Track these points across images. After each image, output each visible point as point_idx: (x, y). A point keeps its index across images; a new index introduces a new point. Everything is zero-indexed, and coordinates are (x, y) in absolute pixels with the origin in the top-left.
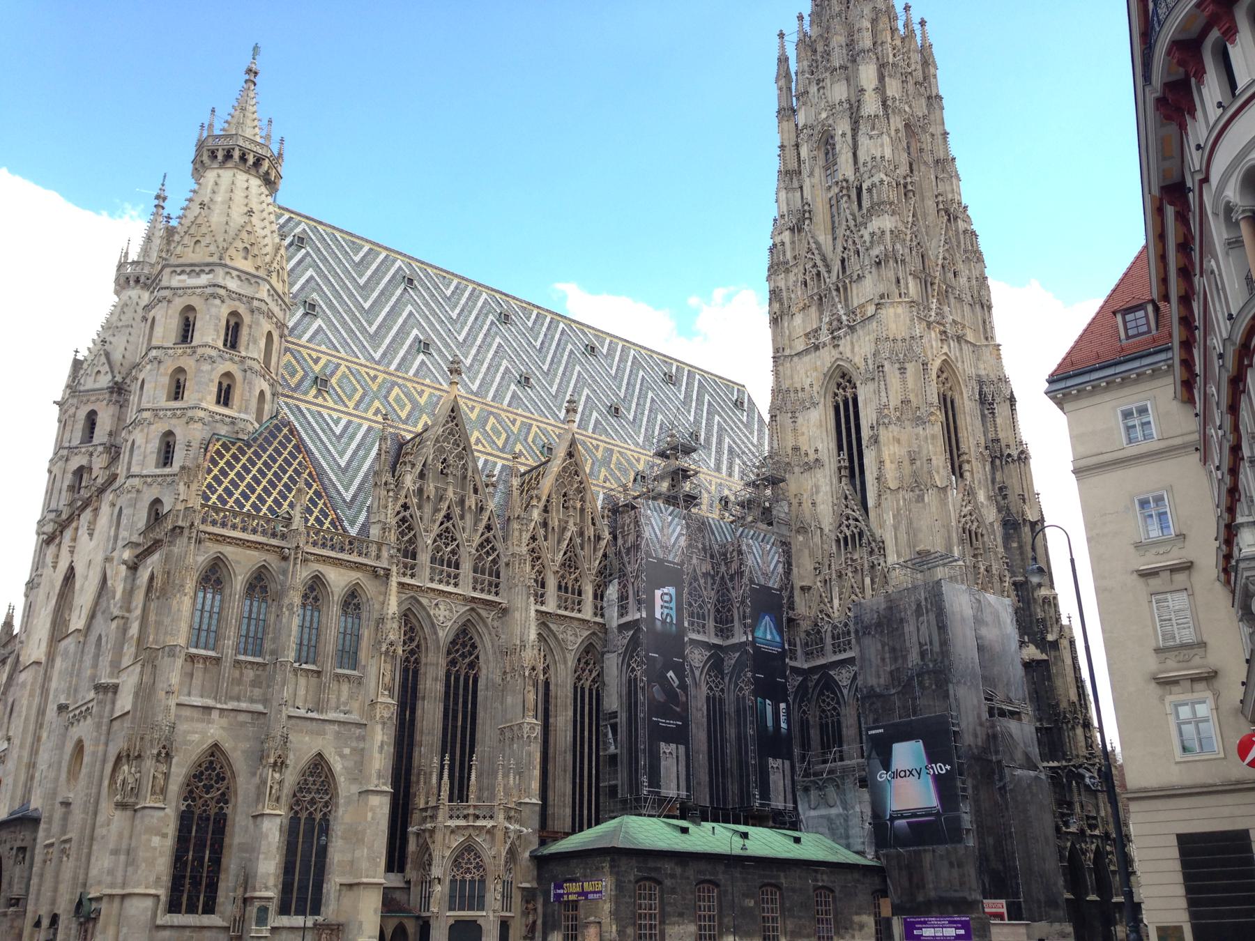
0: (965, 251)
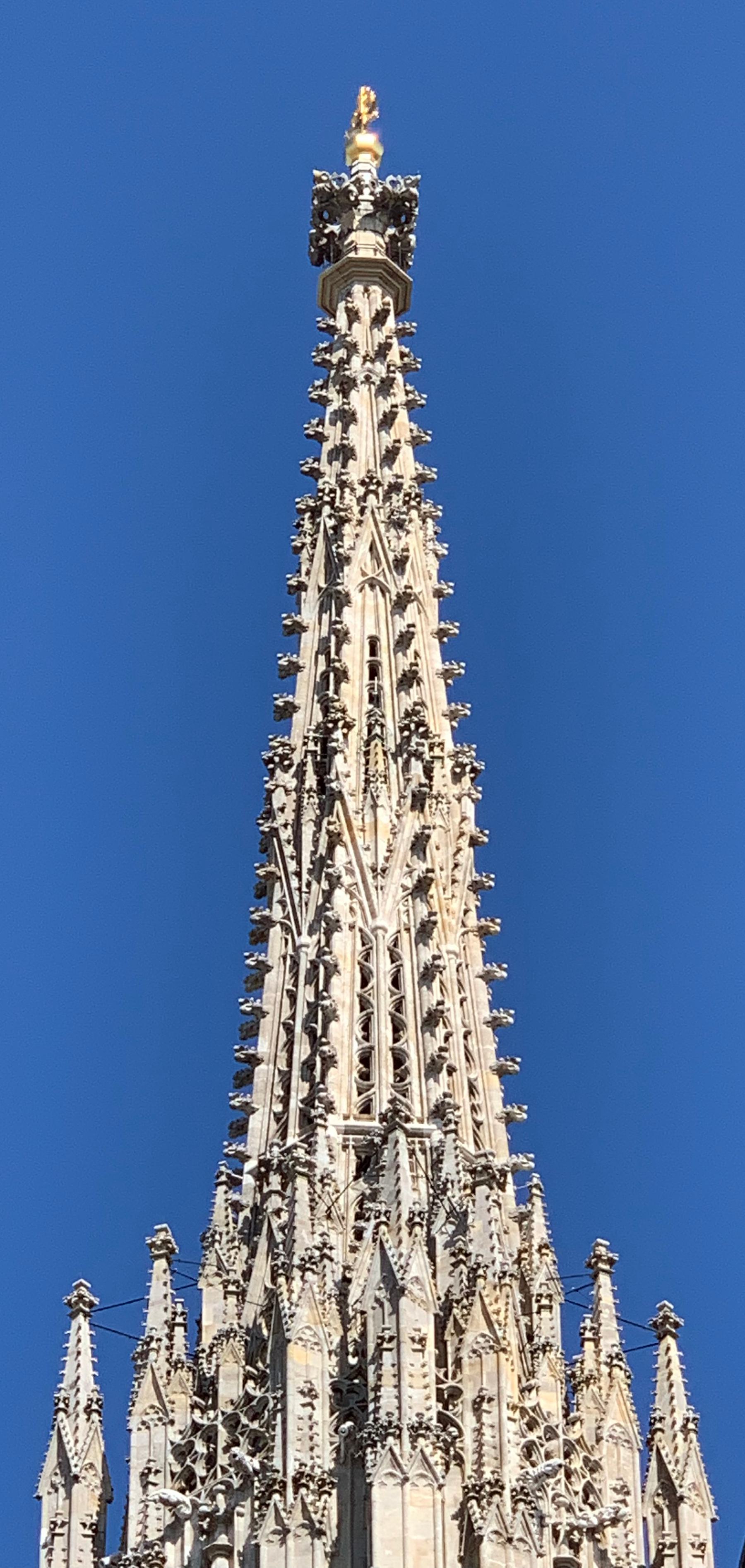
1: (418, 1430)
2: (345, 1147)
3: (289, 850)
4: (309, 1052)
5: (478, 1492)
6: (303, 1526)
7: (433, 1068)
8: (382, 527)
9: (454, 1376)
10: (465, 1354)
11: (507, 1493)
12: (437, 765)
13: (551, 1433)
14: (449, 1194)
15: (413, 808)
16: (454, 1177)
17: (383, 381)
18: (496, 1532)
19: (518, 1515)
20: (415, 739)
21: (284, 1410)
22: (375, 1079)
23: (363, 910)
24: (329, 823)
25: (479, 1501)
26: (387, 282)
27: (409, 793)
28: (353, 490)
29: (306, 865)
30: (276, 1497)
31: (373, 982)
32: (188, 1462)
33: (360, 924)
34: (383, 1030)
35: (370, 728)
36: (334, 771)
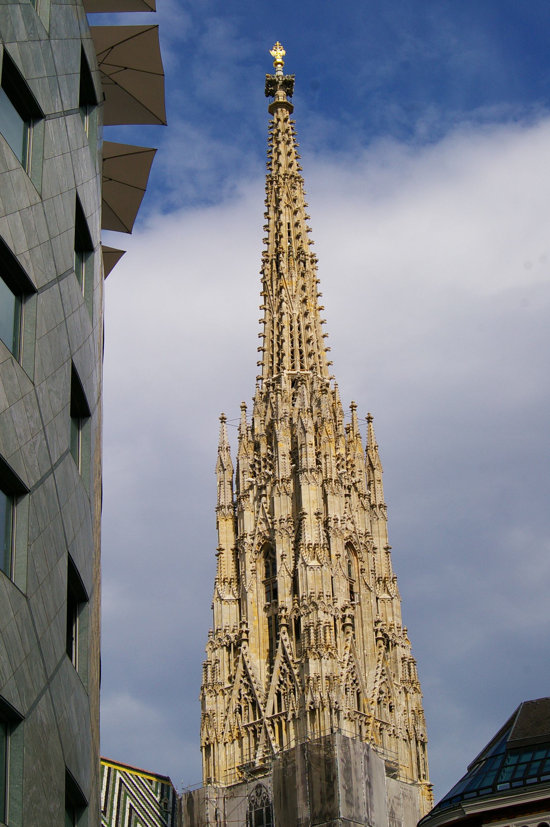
0: (402, 681)
1: (311, 470)
2: (288, 379)
3: (270, 288)
4: (278, 350)
5: (326, 481)
6: (284, 492)
7: (310, 355)
8: (290, 188)
9: (319, 448)
10: (321, 442)
11: (333, 481)
12: (307, 261)
13: (343, 460)
14: (316, 394)
15: (301, 276)
16: (316, 389)
17: (287, 141)
18: (331, 492)
19: (336, 487)
20: (301, 256)
21: (278, 460)
22: (295, 359)
23: (290, 308)
24: (280, 284)
25: (327, 484)
26: (287, 107)
27: (300, 272)
28: (281, 177)
29: (275, 292)
30: (277, 484)
31: (293, 330)
32: (254, 470)
33: (289, 312)
34: (297, 344)
35: (289, 252)
36: (280, 267)
